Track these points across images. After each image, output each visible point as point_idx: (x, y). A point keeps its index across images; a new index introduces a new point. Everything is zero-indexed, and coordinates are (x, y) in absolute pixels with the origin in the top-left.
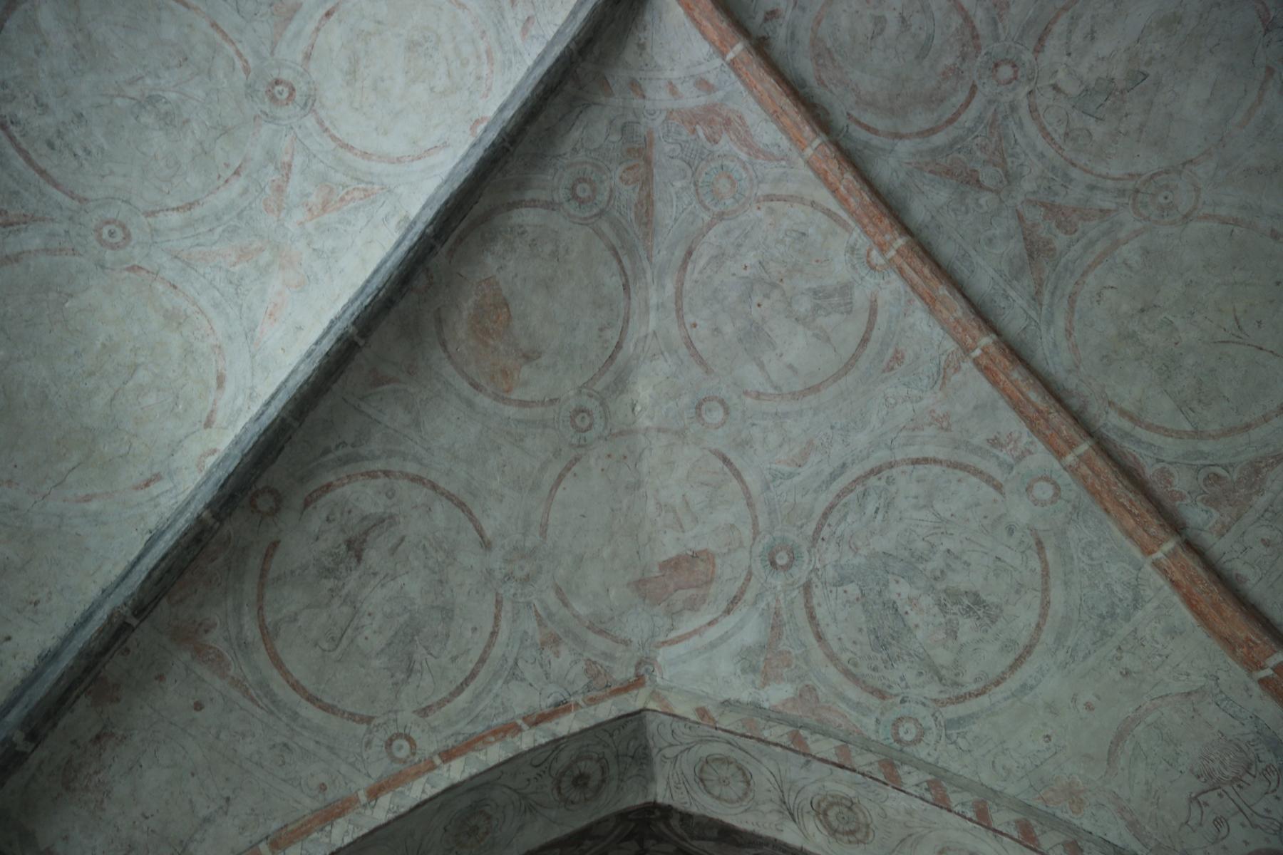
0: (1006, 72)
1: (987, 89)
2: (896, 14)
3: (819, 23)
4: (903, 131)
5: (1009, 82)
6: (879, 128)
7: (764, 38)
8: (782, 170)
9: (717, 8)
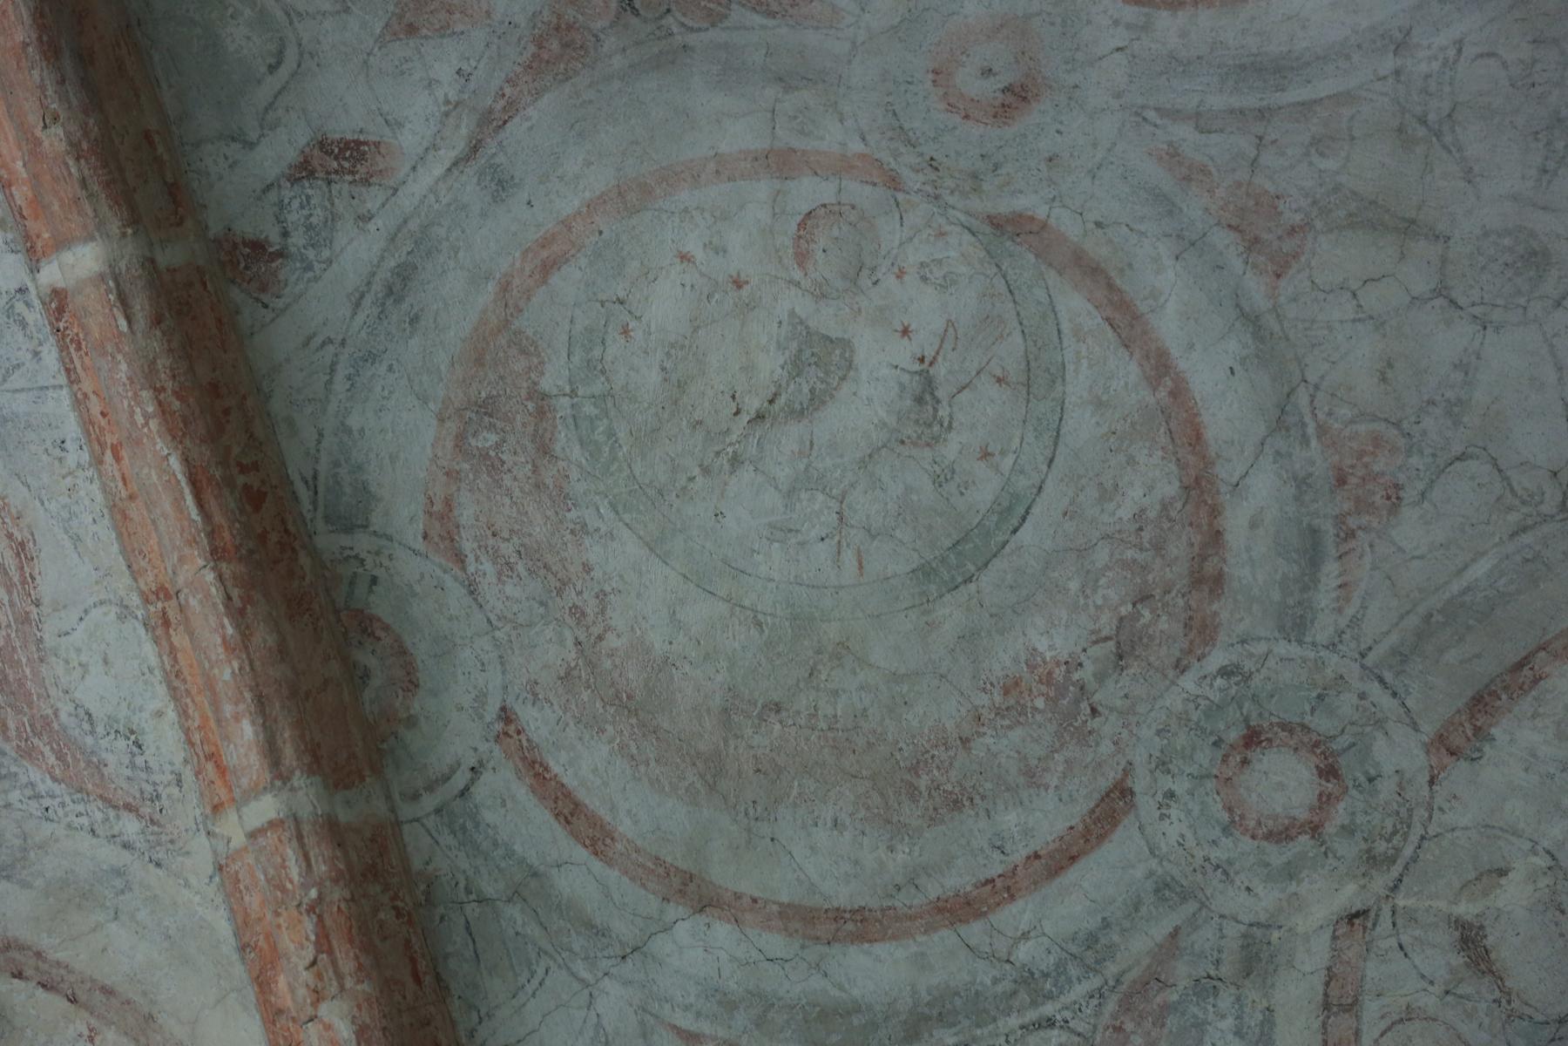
0: (1283, 782)
1: (1169, 829)
2: (903, 353)
3: (547, 269)
4: (724, 874)
5: (1282, 834)
6: (625, 827)
7: (258, 247)
8: (110, 855)
9: (51, 52)
